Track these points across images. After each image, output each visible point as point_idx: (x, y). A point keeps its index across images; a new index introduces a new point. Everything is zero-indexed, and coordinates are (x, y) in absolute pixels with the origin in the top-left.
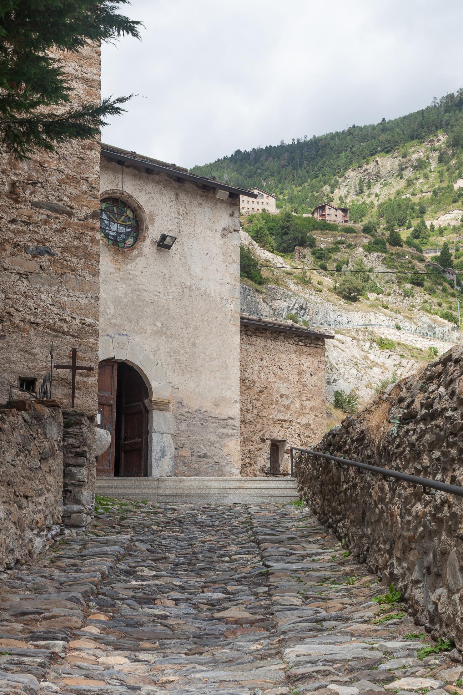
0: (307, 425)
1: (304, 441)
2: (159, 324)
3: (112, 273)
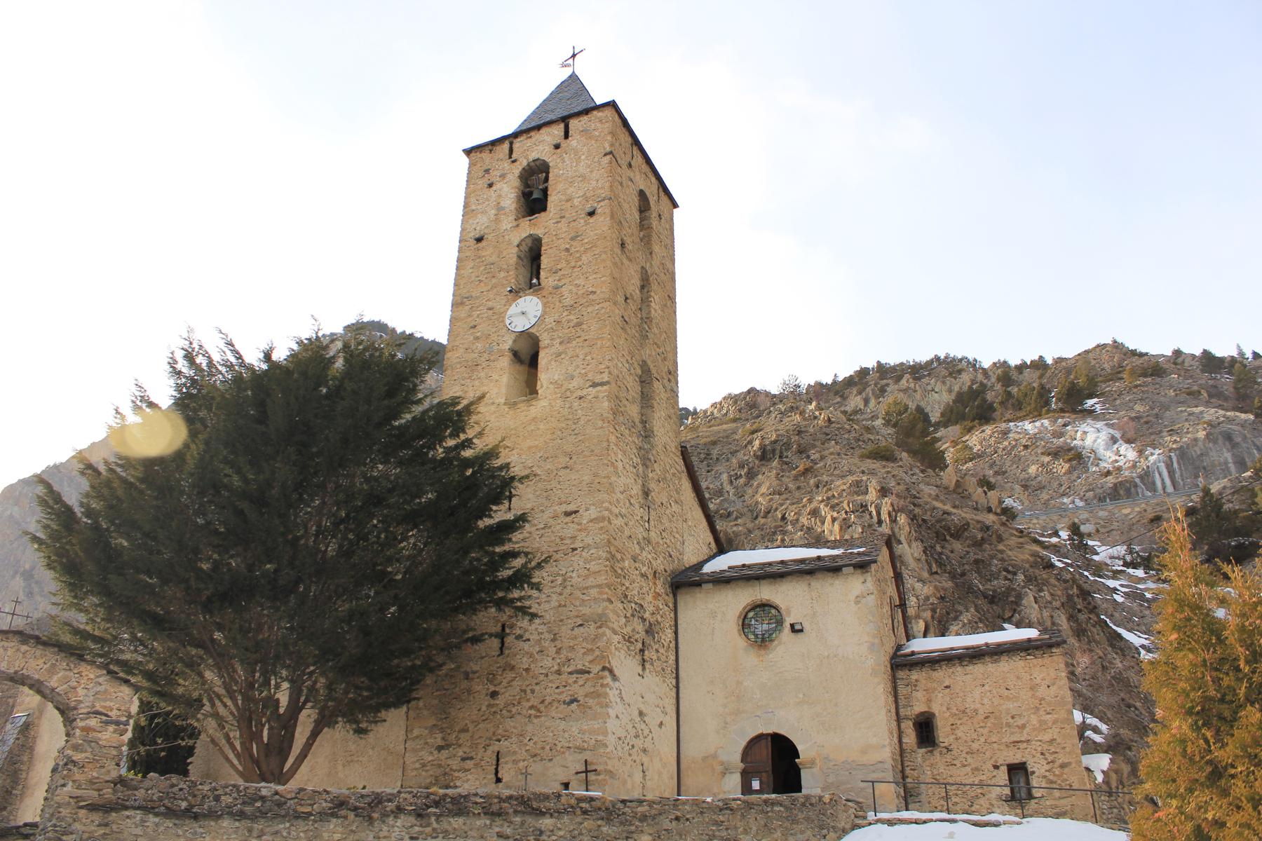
0: (1052, 741)
1: (1050, 758)
2: (801, 696)
3: (756, 666)
